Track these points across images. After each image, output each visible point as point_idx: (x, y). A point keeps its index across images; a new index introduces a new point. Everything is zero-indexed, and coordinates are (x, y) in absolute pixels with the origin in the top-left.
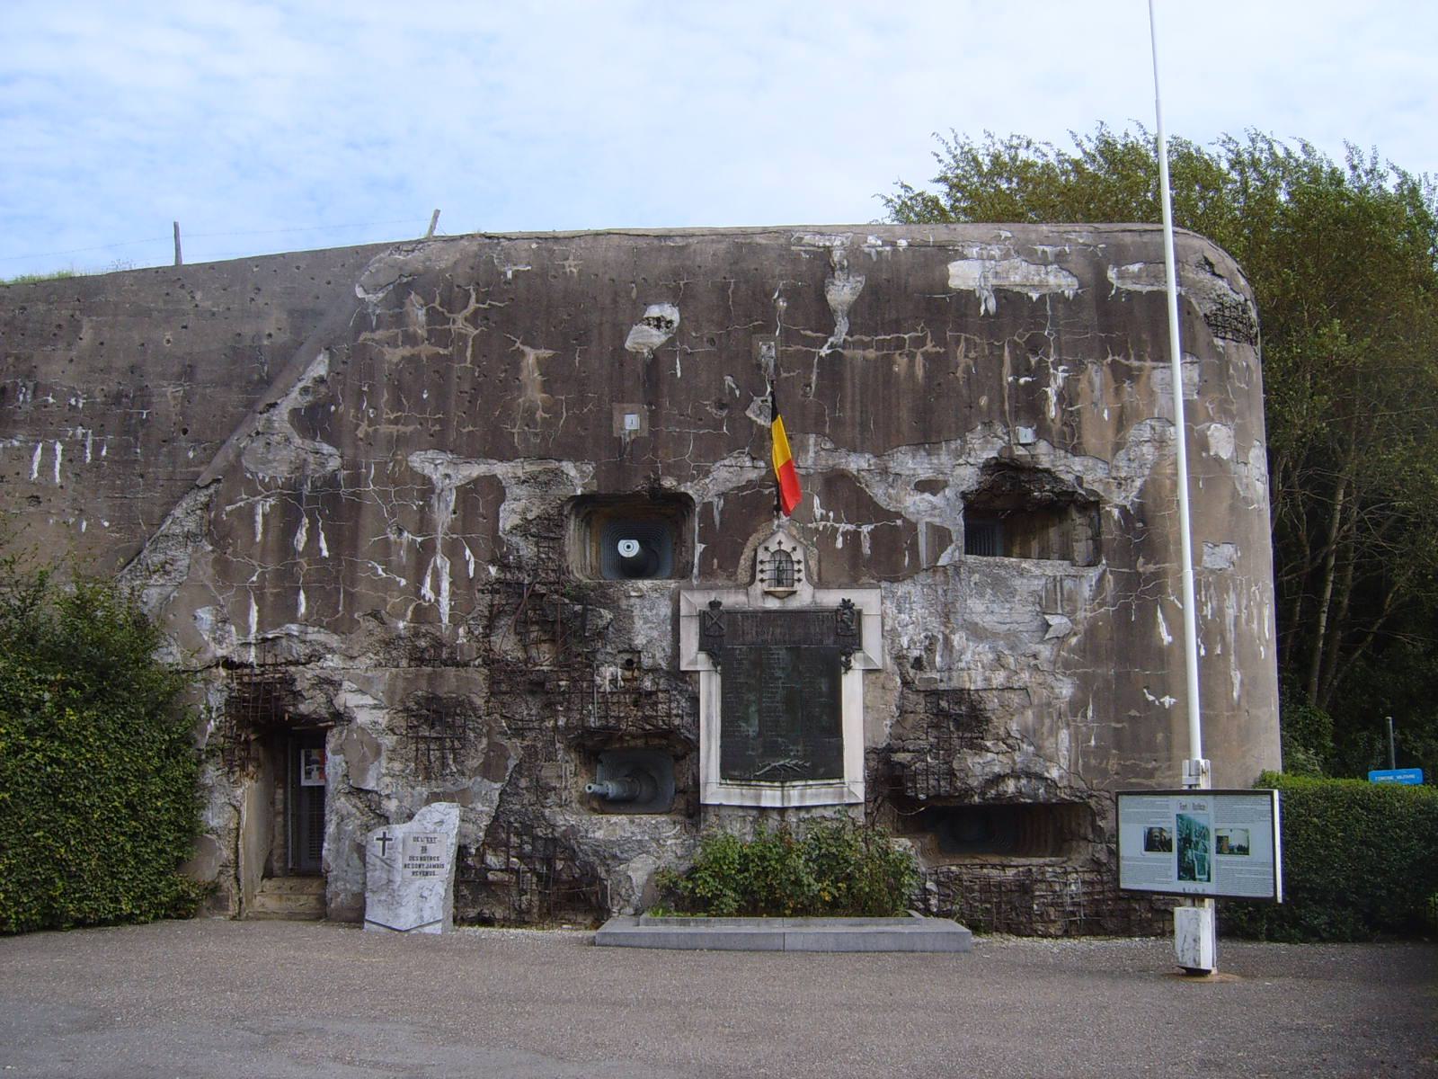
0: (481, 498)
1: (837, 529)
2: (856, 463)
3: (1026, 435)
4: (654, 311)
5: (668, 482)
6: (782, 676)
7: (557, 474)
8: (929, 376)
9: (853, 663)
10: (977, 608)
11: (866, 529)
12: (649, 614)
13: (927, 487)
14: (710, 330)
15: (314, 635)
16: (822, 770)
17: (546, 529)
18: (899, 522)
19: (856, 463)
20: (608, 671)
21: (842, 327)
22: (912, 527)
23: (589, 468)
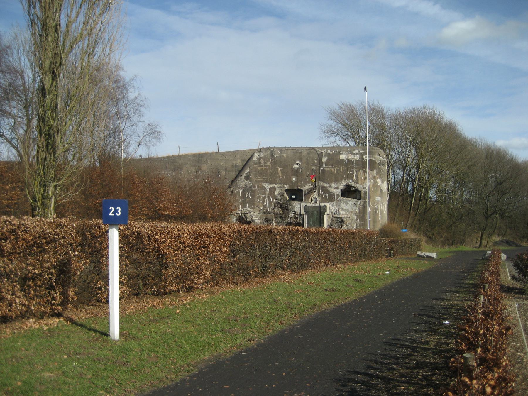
0: (273, 190)
2: (326, 185)
3: (351, 181)
4: (297, 162)
5: (299, 188)
7: (284, 186)
8: (337, 172)
10: (343, 206)
13: (336, 188)
14: (305, 165)
15: (249, 209)
17: (282, 195)
19: (326, 185)
20: (291, 215)
21: (324, 165)
22: (334, 194)
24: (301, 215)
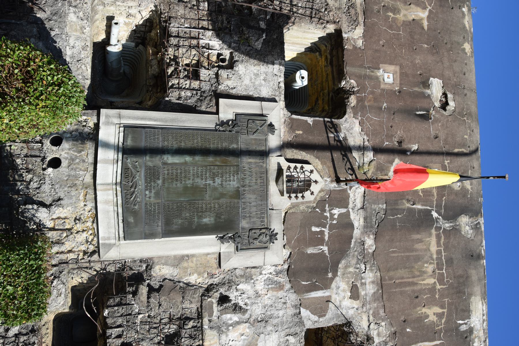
1: (325, 227)
5: (353, 100)
6: (216, 184)
7: (354, 23)
9: (226, 245)
11: (325, 248)
12: (262, 78)
16: (131, 220)
18: (330, 275)
22: (326, 286)
23: (360, 43)
24: (218, 96)
